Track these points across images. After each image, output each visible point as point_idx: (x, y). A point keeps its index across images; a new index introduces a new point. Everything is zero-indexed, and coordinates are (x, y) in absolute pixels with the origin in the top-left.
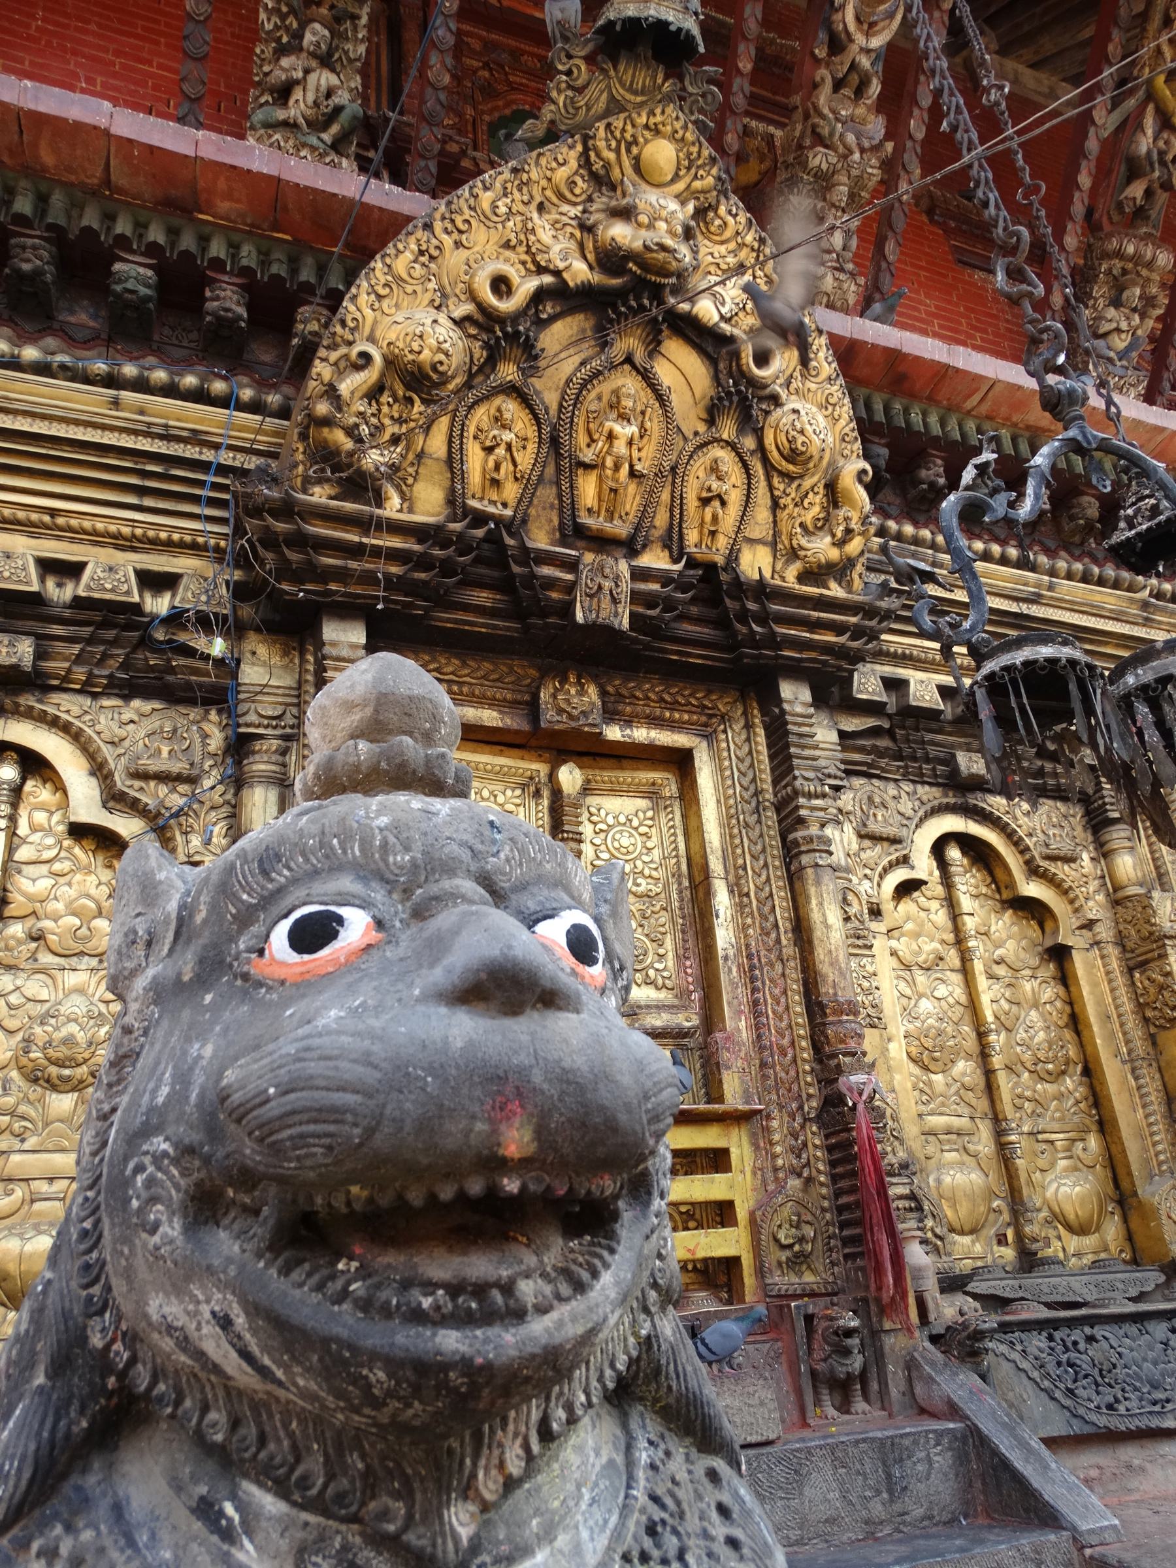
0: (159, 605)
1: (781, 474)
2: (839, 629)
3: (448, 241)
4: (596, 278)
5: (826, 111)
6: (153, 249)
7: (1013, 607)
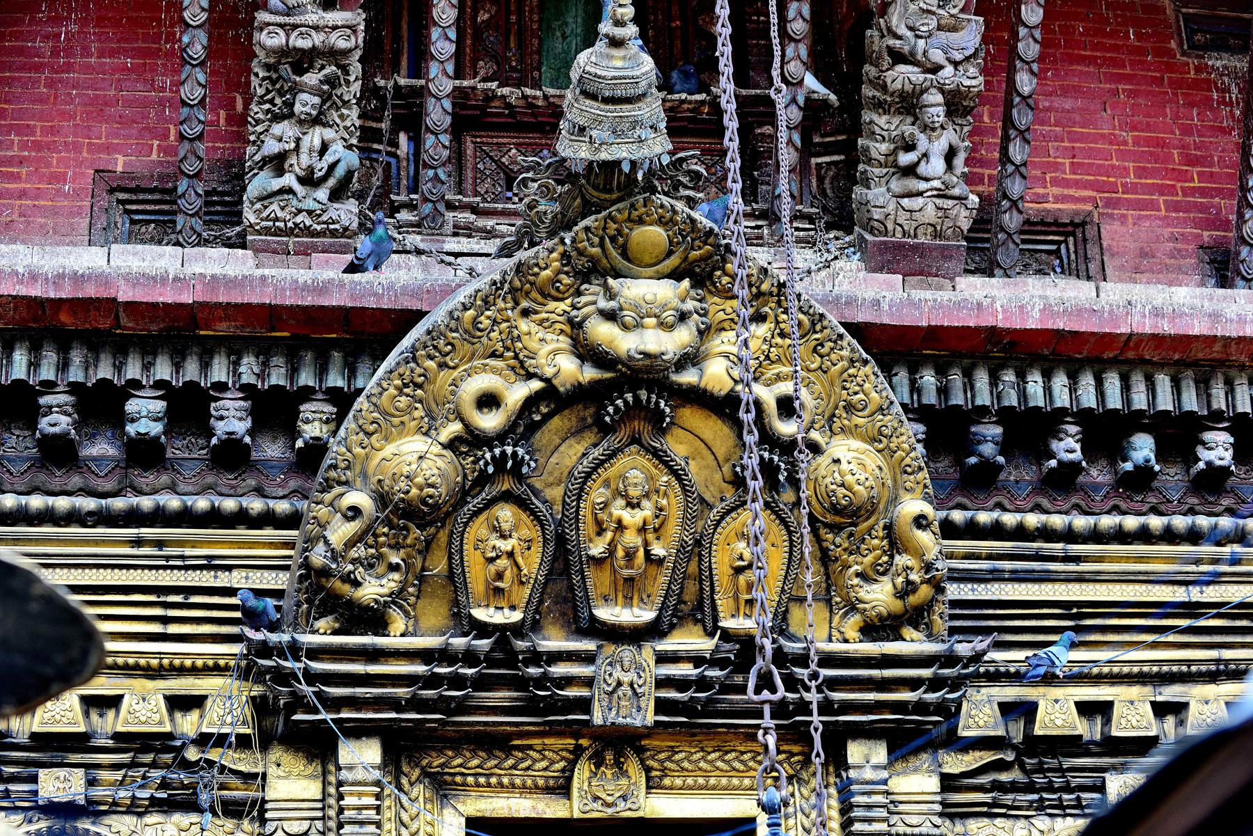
0: (189, 724)
1: (826, 525)
2: (913, 684)
3: (431, 364)
4: (590, 374)
5: (903, 30)
6: (159, 384)
7: (1178, 594)
